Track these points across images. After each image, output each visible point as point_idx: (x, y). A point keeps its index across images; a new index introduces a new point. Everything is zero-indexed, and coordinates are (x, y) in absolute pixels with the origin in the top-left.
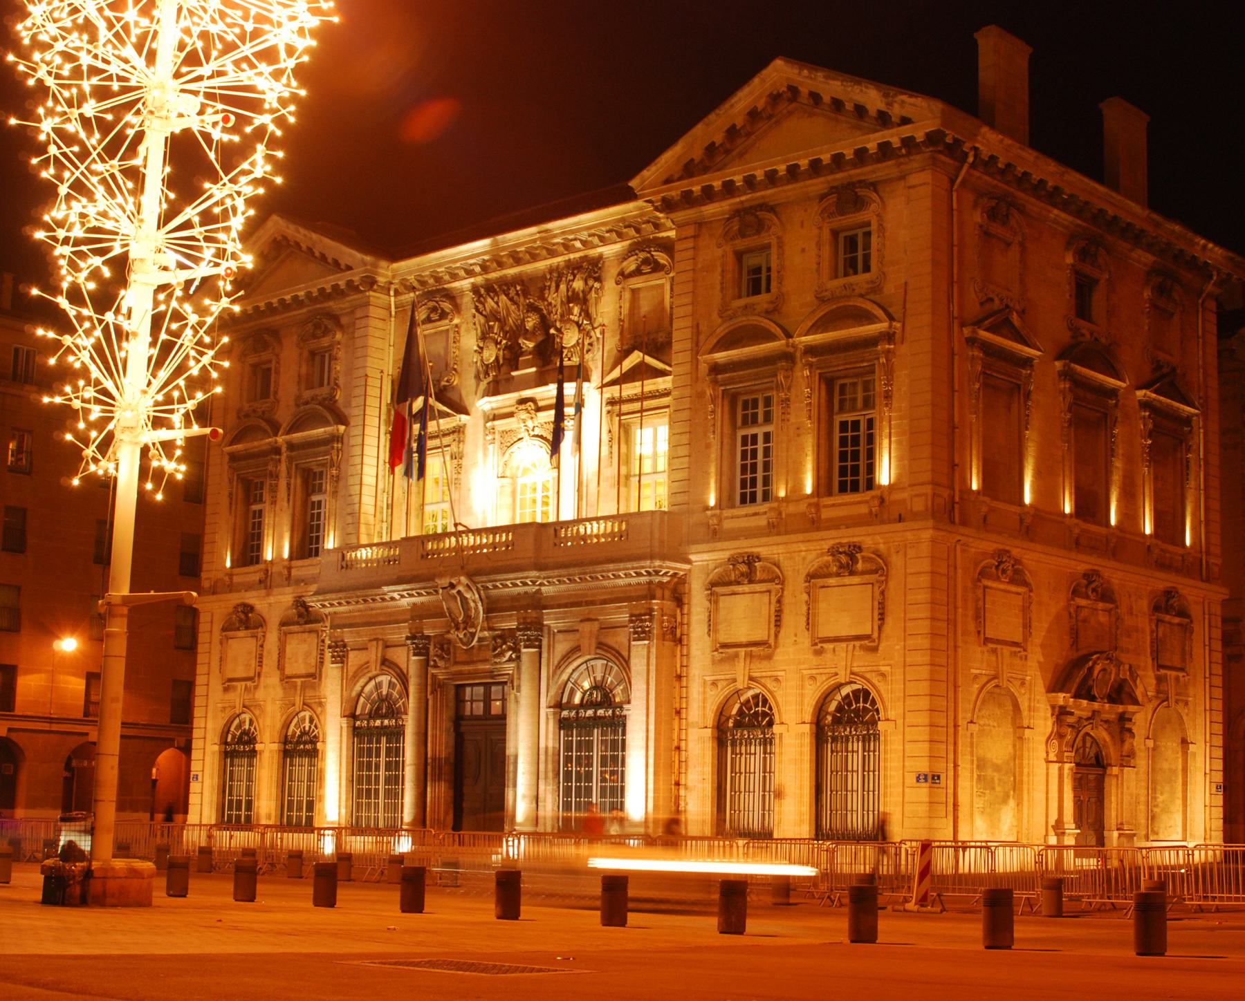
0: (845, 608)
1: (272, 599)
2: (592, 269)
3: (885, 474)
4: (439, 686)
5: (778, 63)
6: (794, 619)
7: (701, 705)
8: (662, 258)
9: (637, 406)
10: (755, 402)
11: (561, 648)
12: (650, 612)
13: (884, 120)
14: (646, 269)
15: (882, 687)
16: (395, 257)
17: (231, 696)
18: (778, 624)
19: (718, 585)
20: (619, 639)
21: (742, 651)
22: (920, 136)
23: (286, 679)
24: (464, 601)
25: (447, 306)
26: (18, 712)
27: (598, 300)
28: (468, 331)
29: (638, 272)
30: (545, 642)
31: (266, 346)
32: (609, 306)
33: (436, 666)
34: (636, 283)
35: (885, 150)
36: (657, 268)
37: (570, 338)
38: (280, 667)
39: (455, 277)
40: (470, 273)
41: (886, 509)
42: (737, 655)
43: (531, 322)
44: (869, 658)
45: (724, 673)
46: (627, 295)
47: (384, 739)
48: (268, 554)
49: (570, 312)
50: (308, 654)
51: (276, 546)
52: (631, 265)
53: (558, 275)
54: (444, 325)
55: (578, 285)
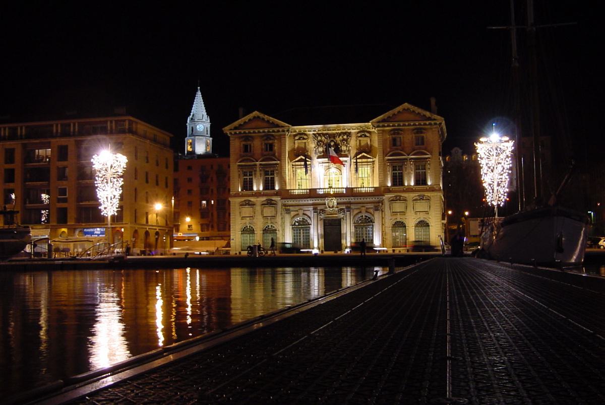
0: (421, 206)
1: (258, 199)
2: (349, 134)
3: (429, 183)
4: (321, 219)
5: (406, 104)
6: (410, 208)
7: (389, 223)
8: (368, 135)
9: (366, 164)
10: (396, 167)
11: (356, 212)
12: (379, 206)
13: (429, 119)
14: (363, 136)
15: (430, 220)
16: (293, 125)
17: (244, 221)
18: (406, 208)
19: (393, 200)
20: (371, 211)
21: (398, 214)
22: (438, 123)
23: (265, 217)
24: (334, 202)
25: (305, 137)
26: (149, 224)
27: (350, 141)
28: (312, 143)
29: (361, 136)
30: (351, 211)
31: (249, 140)
32: (353, 142)
33: (321, 215)
34: (360, 138)
35: (430, 124)
36: (366, 136)
37: (344, 148)
38: (262, 214)
39: (309, 131)
40: (314, 131)
41: (432, 189)
42: (397, 214)
43: (332, 144)
44: (427, 215)
45: (394, 217)
46: (358, 141)
47: (302, 230)
48: (255, 189)
49: (344, 143)
50: (272, 212)
51: (258, 186)
52: (359, 135)
53: (340, 134)
54: (304, 141)
55: (345, 137)
